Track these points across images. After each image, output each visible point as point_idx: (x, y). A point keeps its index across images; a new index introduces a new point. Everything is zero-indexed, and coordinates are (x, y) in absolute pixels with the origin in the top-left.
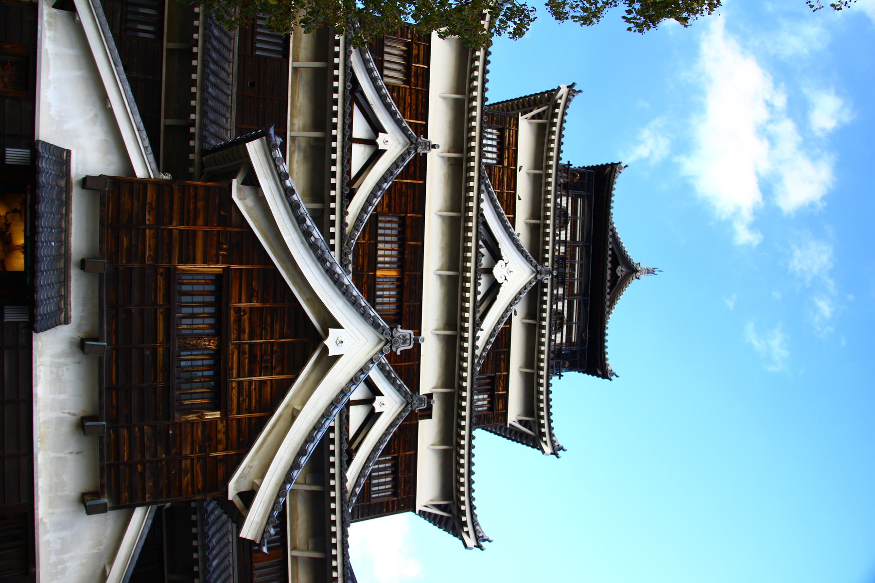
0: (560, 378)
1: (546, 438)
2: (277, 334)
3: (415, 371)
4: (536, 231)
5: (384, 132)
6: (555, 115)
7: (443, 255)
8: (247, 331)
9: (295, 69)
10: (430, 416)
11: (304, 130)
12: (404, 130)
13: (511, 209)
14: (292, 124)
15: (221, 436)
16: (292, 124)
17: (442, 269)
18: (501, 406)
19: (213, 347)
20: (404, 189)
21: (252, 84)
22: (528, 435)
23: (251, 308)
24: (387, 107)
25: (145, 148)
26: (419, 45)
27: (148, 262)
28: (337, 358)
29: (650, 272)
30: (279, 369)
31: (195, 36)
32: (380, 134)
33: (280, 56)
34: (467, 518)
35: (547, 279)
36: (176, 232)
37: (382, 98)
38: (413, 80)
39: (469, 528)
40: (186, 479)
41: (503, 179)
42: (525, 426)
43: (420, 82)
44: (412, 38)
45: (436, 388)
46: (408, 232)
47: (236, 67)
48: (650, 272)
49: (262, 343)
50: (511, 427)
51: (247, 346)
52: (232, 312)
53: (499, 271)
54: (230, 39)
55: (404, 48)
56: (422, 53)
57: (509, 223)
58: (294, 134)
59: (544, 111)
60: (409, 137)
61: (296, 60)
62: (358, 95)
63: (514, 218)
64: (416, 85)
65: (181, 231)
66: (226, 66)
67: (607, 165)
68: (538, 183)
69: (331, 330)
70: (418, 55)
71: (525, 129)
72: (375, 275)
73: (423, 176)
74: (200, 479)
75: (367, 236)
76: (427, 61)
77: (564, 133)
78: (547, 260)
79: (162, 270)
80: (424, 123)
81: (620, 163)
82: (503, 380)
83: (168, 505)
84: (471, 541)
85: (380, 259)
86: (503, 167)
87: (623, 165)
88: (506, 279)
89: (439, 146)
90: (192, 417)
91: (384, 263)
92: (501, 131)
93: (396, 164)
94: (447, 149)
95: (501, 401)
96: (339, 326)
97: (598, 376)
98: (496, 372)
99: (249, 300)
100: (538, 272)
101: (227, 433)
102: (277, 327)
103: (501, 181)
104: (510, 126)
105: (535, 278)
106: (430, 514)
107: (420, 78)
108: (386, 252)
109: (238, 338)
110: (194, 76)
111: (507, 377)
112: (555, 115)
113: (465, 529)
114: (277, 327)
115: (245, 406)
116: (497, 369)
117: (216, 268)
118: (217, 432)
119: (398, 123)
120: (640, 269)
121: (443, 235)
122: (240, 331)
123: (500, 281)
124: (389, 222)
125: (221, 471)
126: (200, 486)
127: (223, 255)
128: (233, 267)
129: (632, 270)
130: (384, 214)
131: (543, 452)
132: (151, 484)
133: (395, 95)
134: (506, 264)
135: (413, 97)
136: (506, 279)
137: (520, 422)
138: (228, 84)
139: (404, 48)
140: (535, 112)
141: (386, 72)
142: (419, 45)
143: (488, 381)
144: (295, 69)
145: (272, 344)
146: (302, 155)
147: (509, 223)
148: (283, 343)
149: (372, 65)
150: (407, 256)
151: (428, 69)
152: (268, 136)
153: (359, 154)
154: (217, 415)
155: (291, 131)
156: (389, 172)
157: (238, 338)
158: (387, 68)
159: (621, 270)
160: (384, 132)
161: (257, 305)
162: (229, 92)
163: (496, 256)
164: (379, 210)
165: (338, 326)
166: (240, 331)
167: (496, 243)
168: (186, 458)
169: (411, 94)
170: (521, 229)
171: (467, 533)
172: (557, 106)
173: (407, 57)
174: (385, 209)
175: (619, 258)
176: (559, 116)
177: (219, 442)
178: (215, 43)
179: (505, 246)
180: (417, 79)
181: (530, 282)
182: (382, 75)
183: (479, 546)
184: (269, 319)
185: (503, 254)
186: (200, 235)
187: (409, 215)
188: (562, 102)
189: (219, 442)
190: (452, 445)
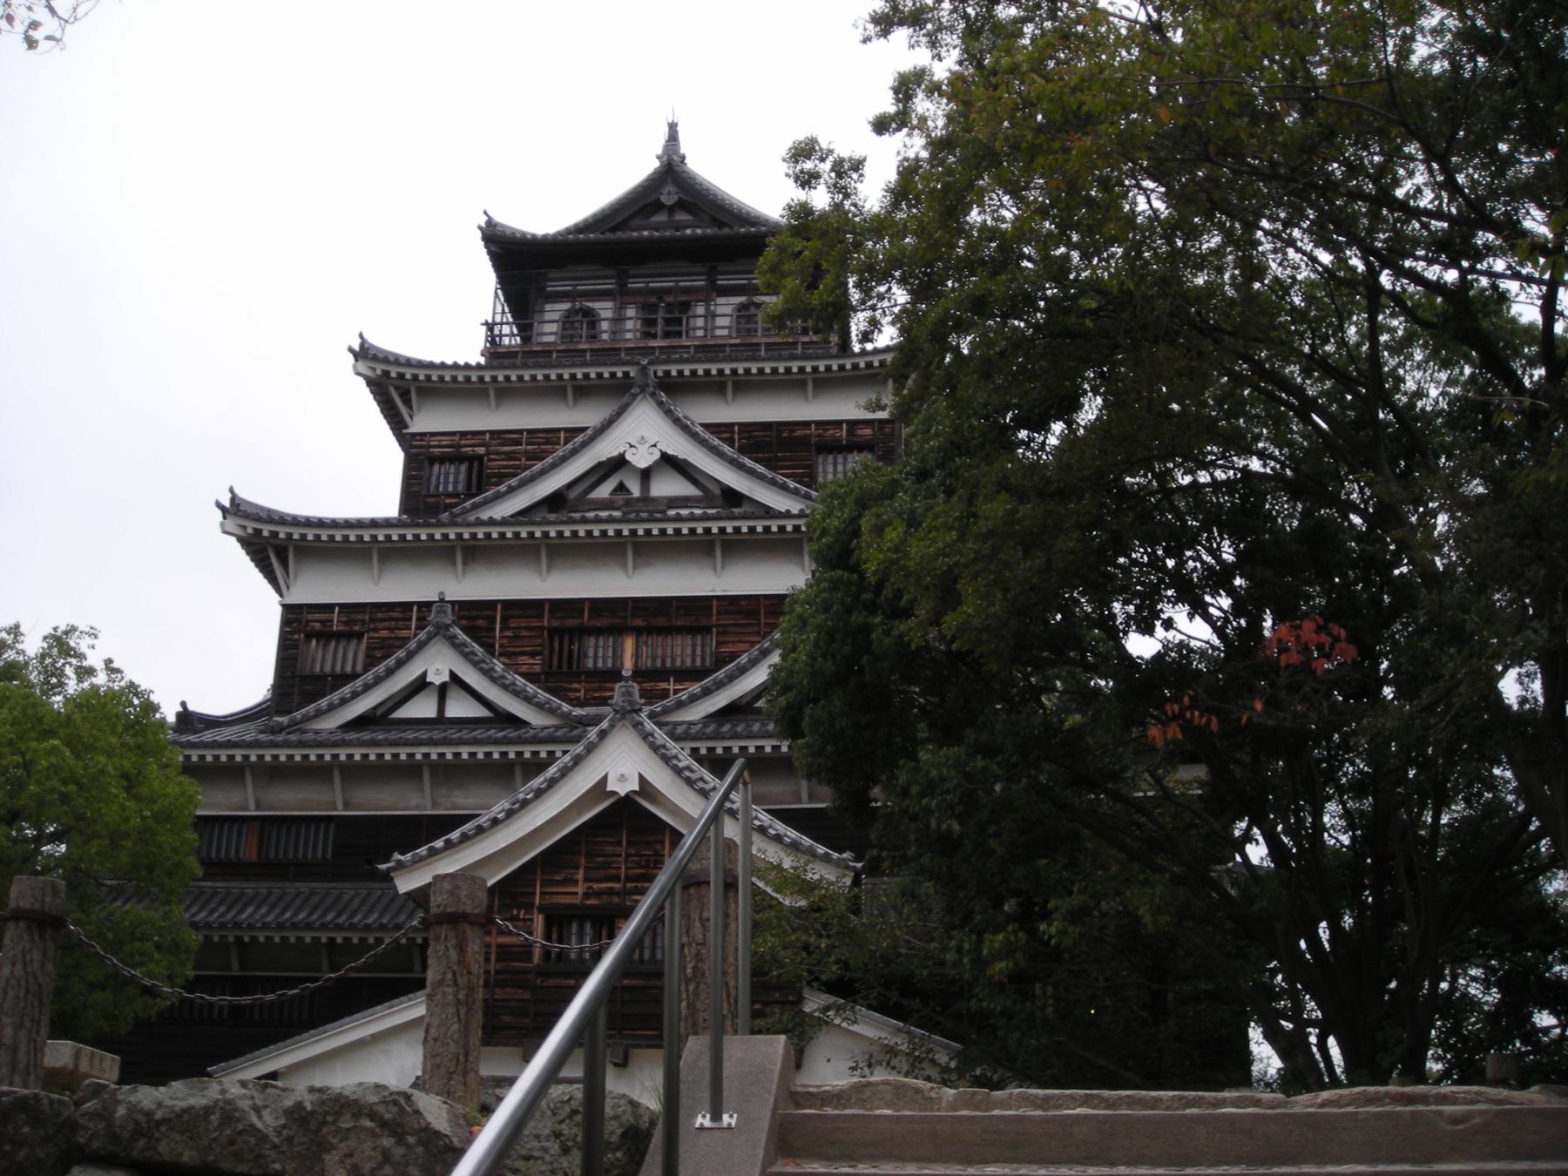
3: (774, 602)
4: (583, 391)
5: (425, 674)
6: (401, 376)
8: (610, 885)
9: (347, 806)
12: (421, 646)
13: (549, 437)
14: (417, 808)
16: (417, 808)
17: (625, 566)
18: (868, 431)
20: (509, 634)
23: (586, 880)
24: (390, 672)
25: (410, 1000)
27: (527, 996)
28: (642, 779)
29: (673, 137)
30: (658, 847)
31: (308, 940)
32: (428, 680)
33: (332, 826)
35: (655, 372)
36: (499, 966)
37: (379, 681)
38: (356, 628)
41: (505, 453)
43: (360, 617)
44: (299, 632)
45: (803, 565)
46: (571, 623)
47: (348, 885)
48: (673, 137)
49: (627, 868)
51: (629, 885)
52: (589, 902)
54: (312, 893)
55: (314, 642)
57: (577, 438)
58: (429, 804)
59: (397, 388)
60: (430, 638)
62: (379, 712)
63: (567, 430)
64: (363, 622)
65: (497, 960)
66: (346, 897)
67: (486, 246)
68: (506, 393)
69: (610, 788)
70: (322, 622)
71: (430, 420)
73: (490, 605)
75: (576, 686)
76: (329, 607)
78: (626, 374)
79: (539, 982)
80: (415, 608)
81: (480, 228)
85: (610, 665)
87: (482, 221)
88: (655, 446)
89: (441, 593)
91: (614, 657)
92: (433, 460)
93: (468, 656)
95: (859, 432)
96: (605, 777)
100: (643, 389)
102: (609, 849)
103: (510, 456)
105: (653, 395)
107: (354, 616)
109: (618, 894)
110: (355, 941)
111: (819, 424)
112: (401, 376)
114: (609, 849)
116: (803, 443)
117: (539, 922)
119: (411, 655)
120: (665, 158)
123: (657, 456)
127: (525, 914)
128: (537, 902)
129: (671, 171)
132: (777, 994)
133: (378, 654)
134: (631, 446)
135: (379, 625)
136: (655, 446)
138: (369, 895)
139: (314, 642)
141: (349, 668)
142: (308, 621)
144: (347, 806)
145: (628, 855)
147: (577, 438)
148: (628, 842)
149: (335, 697)
151: (342, 606)
152: (390, 869)
153: (459, 707)
155: (425, 809)
156: (476, 664)
157: (618, 894)
158: (342, 667)
159: (669, 196)
160: (425, 674)
161: (581, 872)
162: (379, 893)
163: (619, 463)
164: (538, 669)
165: (604, 780)
166: (610, 892)
167: (600, 465)
169: (376, 630)
170: (586, 416)
172: (386, 374)
173: (325, 636)
174: (538, 660)
175: (648, 202)
176: (401, 370)
178: (315, 917)
179: (605, 449)
180: (355, 622)
181: (660, 404)
182: (354, 676)
185: (615, 453)
186: (501, 940)
187: (546, 624)
188: (380, 368)
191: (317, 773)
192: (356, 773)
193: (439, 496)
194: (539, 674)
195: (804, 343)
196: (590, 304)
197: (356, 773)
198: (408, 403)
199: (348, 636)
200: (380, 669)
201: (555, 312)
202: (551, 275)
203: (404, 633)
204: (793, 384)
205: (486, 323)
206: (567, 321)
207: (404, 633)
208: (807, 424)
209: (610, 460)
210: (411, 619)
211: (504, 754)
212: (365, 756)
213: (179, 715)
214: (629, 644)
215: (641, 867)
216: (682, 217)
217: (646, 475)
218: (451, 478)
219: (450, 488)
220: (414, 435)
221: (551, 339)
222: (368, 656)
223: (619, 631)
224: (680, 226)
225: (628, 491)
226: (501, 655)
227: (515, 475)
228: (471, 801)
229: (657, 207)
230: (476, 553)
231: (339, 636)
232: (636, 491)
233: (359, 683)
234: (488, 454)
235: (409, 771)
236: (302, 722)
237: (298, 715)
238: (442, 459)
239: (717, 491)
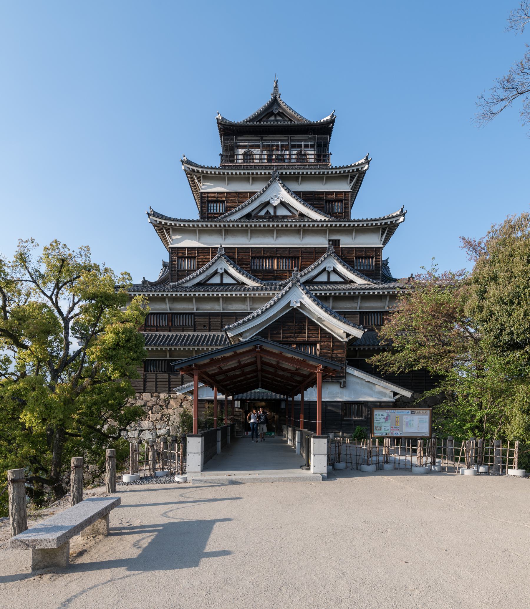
0: (332, 154)
1: (360, 167)
2: (291, 324)
5: (217, 270)
7: (267, 237)
10: (339, 241)
11: (220, 305)
15: (326, 344)
16: (218, 310)
17: (273, 237)
18: (341, 195)
19: (295, 346)
21: (205, 326)
22: (358, 177)
26: (178, 253)
30: (304, 323)
34: (389, 221)
37: (204, 271)
38: (193, 255)
39: (394, 220)
40: (339, 355)
41: (231, 200)
42: (352, 181)
44: (175, 256)
46: (258, 255)
49: (295, 330)
50: (353, 187)
53: (276, 203)
56: (181, 251)
59: (196, 176)
61: (193, 309)
63: (250, 192)
64: (195, 253)
70: (182, 253)
72: (276, 270)
74: (339, 351)
75: (260, 274)
77: (206, 166)
82: (328, 195)
83: (347, 362)
84: (402, 219)
86: (226, 200)
90: (318, 353)
92: (209, 202)
94: (221, 237)
97: (333, 125)
98: (324, 199)
99: (280, 334)
101: (325, 342)
103: (233, 201)
104: (206, 197)
106: (384, 240)
108: (266, 264)
113: (394, 222)
114: (290, 324)
115: (316, 335)
116: (321, 199)
118: (324, 345)
121: (258, 237)
122: (291, 337)
123: (279, 202)
124: (254, 264)
125: (338, 344)
126: (342, 351)
130: (251, 267)
131: (367, 169)
133: (201, 264)
137: (350, 183)
140: (196, 181)
143: (328, 204)
144: (197, 310)
146: (229, 306)
150: (269, 255)
151: (188, 248)
153: (227, 280)
154: (318, 345)
160: (217, 270)
163: (268, 203)
164: (249, 269)
168: (332, 355)
169: (200, 256)
171: (396, 221)
174: (249, 266)
175: (268, 112)
177: (328, 345)
179: (264, 199)
183: (404, 214)
184: (287, 327)
185: (267, 200)
189: (328, 345)
190: (353, 229)
191: (189, 300)
192: (199, 300)
193: (212, 214)
194: (249, 270)
195: (320, 165)
196: (252, 150)
197: (199, 300)
198: (199, 181)
199: (191, 258)
200: (204, 268)
201: (241, 151)
202: (239, 138)
203: (208, 257)
204: (319, 178)
205: (221, 155)
206: (245, 155)
207: (208, 257)
208: (323, 192)
209: (265, 202)
210: (210, 253)
211: (245, 294)
212: (204, 295)
213: (143, 282)
214: (276, 261)
215: (299, 329)
216: (279, 118)
217: (275, 208)
218: (215, 208)
219: (215, 211)
220: (202, 193)
221: (240, 161)
222: (198, 265)
223: (272, 258)
224: (277, 121)
225: (270, 213)
226: (237, 264)
227: (235, 208)
228: (234, 308)
229: (272, 114)
230: (228, 231)
231: (188, 258)
232: (272, 214)
233: (198, 272)
234: (226, 200)
235: (216, 299)
236: (181, 284)
237: (180, 282)
238: (212, 202)
239: (297, 214)
